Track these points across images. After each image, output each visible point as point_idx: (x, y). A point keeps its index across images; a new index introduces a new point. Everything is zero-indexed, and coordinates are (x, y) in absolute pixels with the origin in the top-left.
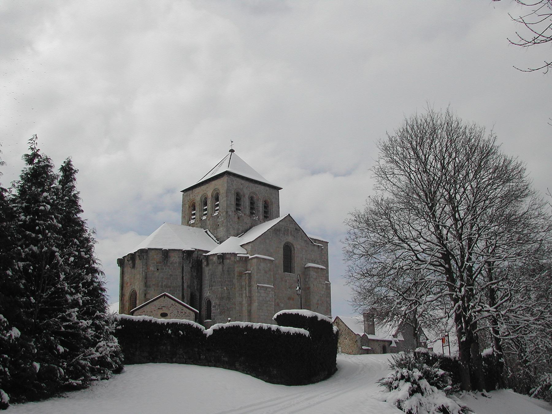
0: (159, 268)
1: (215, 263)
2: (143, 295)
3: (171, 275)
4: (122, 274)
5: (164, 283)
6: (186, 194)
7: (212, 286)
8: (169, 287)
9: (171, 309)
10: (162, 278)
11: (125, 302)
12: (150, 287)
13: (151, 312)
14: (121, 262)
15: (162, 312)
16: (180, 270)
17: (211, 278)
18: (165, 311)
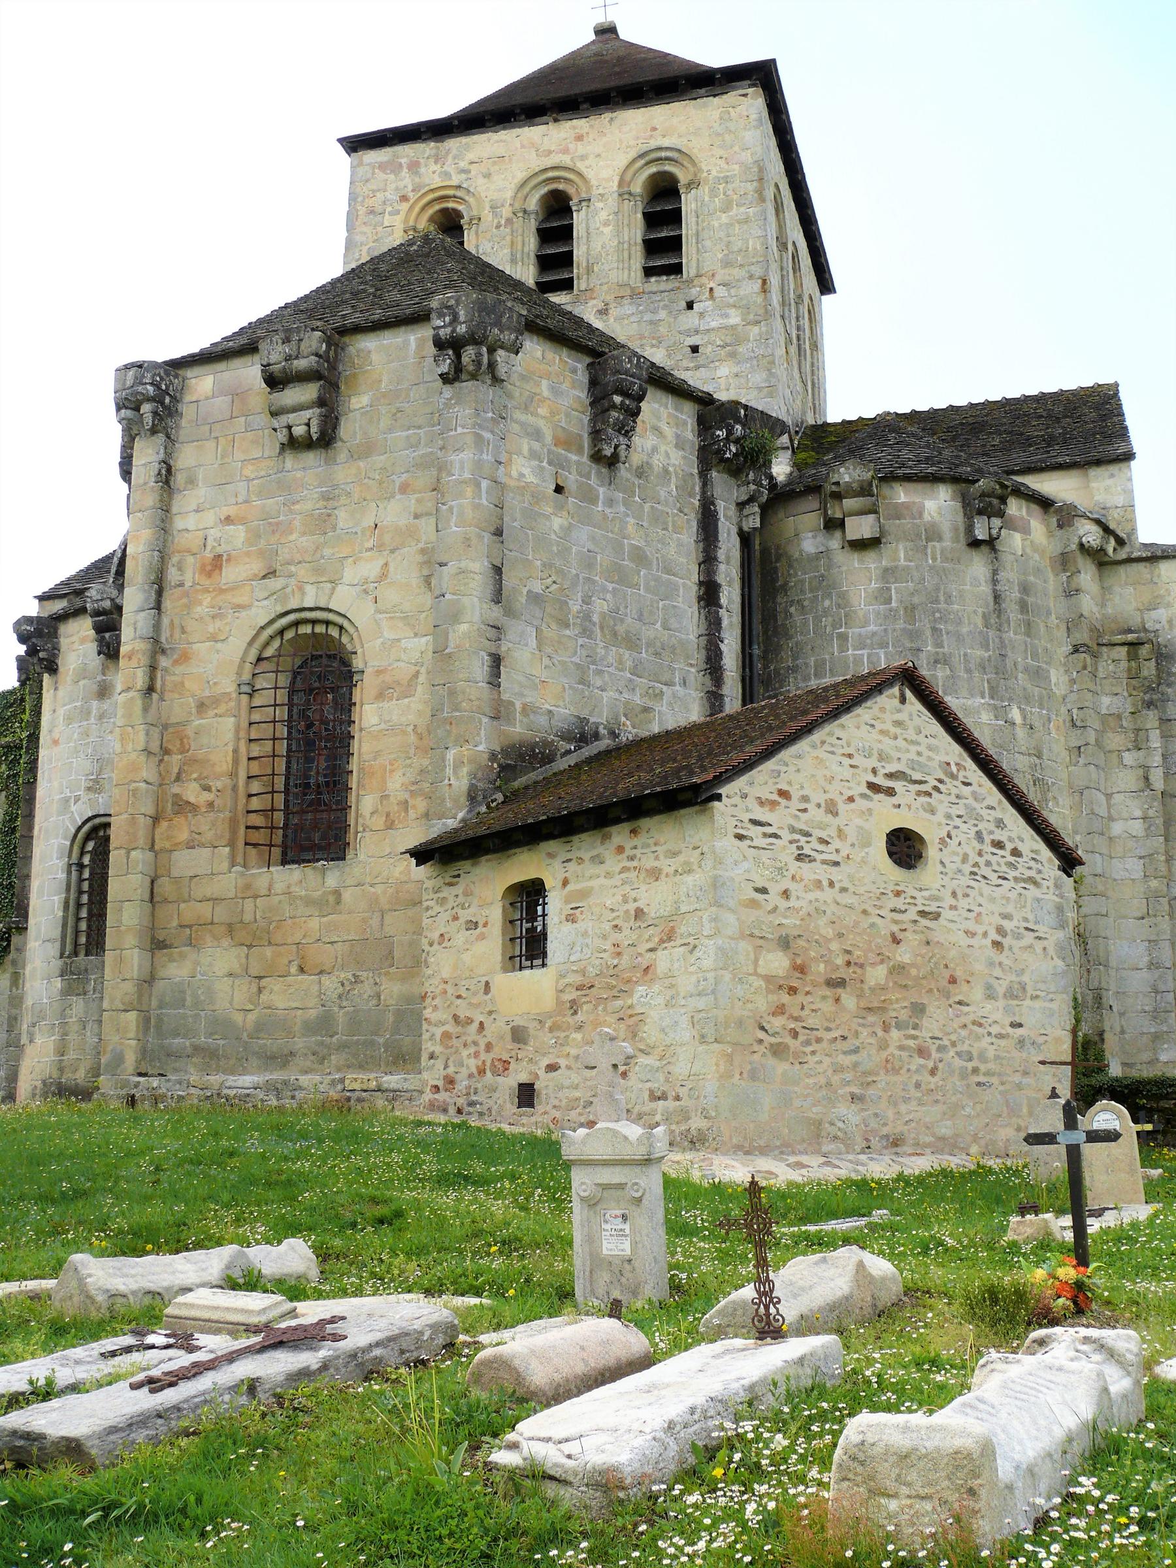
0: (571, 480)
1: (933, 534)
3: (640, 557)
5: (600, 606)
6: (373, 157)
8: (631, 642)
11: (178, 707)
13: (831, 809)
14: (152, 401)
16: (687, 535)
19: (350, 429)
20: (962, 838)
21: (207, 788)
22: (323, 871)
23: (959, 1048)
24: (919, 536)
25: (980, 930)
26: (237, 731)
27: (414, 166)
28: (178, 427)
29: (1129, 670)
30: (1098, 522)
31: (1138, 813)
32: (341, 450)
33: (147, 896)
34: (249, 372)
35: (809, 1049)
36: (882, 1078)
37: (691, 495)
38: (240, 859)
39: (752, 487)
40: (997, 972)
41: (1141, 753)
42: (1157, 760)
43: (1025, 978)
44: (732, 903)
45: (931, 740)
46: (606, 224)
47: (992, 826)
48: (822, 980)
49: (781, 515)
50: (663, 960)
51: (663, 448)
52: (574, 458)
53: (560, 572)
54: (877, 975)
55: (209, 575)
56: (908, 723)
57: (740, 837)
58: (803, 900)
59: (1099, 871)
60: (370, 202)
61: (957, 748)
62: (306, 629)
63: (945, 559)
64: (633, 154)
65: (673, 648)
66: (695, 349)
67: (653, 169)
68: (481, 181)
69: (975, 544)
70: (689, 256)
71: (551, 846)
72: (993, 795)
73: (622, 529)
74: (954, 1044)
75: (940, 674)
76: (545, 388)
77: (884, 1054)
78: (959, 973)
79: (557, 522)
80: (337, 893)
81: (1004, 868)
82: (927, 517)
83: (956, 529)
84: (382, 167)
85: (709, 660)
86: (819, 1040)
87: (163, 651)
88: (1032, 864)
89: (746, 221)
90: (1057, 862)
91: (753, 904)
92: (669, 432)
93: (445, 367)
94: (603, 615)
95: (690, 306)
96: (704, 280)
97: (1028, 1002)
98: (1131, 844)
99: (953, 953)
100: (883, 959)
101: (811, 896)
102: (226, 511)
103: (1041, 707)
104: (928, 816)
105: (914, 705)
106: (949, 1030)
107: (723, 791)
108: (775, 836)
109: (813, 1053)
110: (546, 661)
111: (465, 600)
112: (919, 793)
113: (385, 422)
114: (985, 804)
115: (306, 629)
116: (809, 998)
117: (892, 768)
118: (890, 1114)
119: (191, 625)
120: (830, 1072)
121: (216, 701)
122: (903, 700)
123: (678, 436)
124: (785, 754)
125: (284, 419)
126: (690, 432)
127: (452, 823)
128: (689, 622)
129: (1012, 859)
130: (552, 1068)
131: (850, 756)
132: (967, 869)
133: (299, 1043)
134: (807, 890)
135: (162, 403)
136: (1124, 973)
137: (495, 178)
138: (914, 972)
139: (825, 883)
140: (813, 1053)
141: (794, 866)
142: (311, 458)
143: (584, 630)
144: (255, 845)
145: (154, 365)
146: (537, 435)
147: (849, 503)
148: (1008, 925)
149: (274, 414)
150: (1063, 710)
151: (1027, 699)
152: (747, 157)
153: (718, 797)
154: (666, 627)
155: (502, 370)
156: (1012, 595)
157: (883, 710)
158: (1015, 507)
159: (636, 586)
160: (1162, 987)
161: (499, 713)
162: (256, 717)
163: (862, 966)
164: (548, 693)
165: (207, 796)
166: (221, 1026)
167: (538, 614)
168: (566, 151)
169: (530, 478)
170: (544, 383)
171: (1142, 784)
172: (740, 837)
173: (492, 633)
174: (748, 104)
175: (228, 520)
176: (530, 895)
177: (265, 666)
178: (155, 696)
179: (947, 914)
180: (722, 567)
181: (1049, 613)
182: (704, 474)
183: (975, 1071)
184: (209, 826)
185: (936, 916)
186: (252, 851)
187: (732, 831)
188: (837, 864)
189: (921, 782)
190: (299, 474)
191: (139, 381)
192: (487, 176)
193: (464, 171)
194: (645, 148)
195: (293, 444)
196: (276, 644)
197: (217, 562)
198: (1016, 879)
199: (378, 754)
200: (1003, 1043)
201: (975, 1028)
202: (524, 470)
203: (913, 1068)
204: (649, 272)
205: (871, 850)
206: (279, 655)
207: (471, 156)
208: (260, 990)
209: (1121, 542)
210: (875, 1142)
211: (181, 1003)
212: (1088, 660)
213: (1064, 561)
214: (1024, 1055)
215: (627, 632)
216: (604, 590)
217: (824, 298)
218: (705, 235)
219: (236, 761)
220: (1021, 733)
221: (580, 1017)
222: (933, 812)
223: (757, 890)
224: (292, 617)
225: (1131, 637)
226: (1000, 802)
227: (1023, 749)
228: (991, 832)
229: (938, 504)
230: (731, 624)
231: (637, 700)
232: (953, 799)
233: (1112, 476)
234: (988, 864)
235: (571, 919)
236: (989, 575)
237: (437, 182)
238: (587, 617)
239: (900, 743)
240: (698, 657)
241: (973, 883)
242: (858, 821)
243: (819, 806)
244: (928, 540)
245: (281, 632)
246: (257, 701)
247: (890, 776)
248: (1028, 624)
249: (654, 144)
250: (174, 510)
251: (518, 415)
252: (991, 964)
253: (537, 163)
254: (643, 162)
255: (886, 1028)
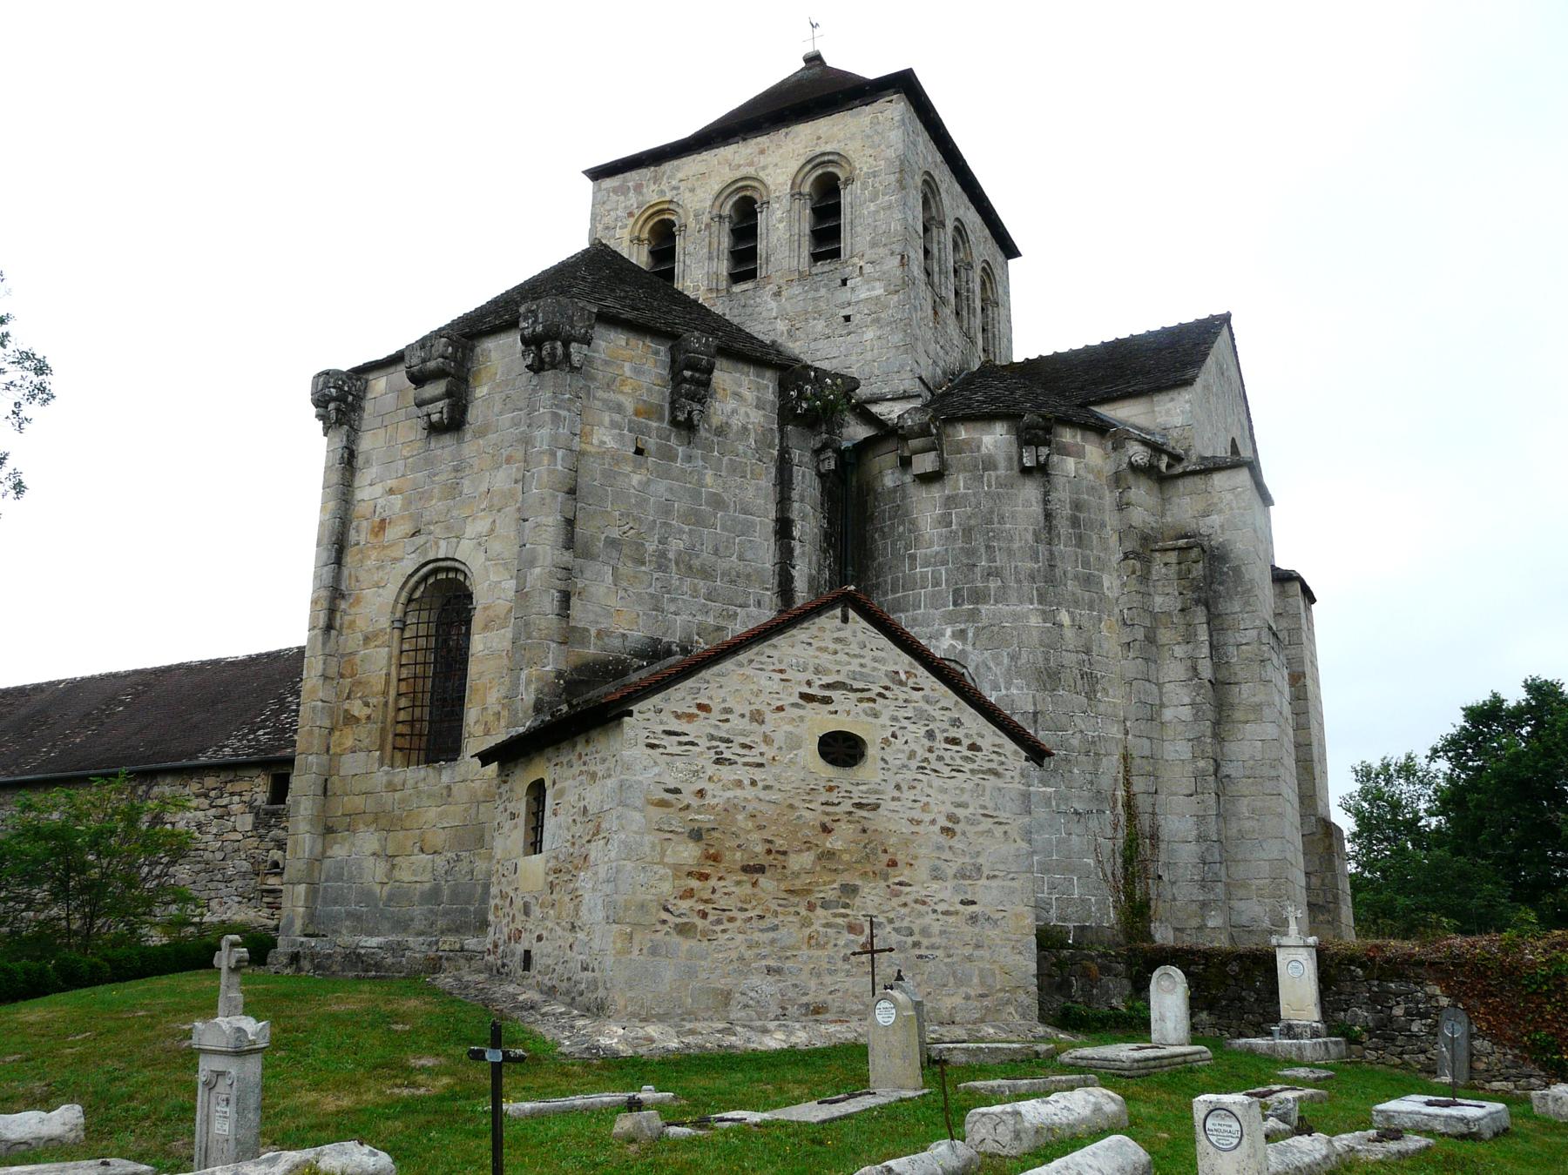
0: (651, 443)
1: (989, 464)
2: (548, 603)
3: (717, 502)
4: (347, 464)
5: (676, 545)
6: (609, 183)
7: (978, 597)
8: (706, 573)
9: (886, 709)
10: (666, 509)
11: (351, 641)
12: (587, 554)
13: (757, 717)
14: (340, 399)
15: (833, 726)
16: (766, 481)
17: (970, 553)
18: (846, 717)
19: (475, 414)
20: (910, 737)
21: (367, 705)
22: (440, 771)
23: (897, 925)
24: (976, 466)
25: (927, 818)
26: (390, 658)
27: (638, 188)
28: (361, 418)
29: (1180, 572)
30: (1145, 443)
31: (1187, 700)
32: (469, 431)
33: (320, 792)
34: (399, 375)
35: (719, 928)
36: (805, 952)
37: (771, 446)
38: (387, 761)
39: (825, 436)
40: (947, 855)
41: (1190, 646)
42: (1205, 651)
43: (980, 860)
44: (638, 803)
45: (877, 653)
46: (780, 221)
47: (946, 726)
48: (738, 867)
49: (870, 455)
50: (595, 850)
51: (742, 410)
52: (655, 424)
53: (637, 519)
54: (801, 861)
55: (376, 535)
56: (851, 639)
57: (652, 746)
58: (718, 796)
59: (1147, 753)
60: (606, 220)
61: (906, 658)
62: (442, 576)
63: (1000, 485)
64: (803, 161)
65: (749, 575)
66: (847, 319)
67: (820, 171)
68: (687, 194)
69: (1026, 471)
70: (846, 243)
71: (549, 752)
72: (948, 696)
73: (699, 480)
74: (891, 921)
75: (992, 585)
76: (627, 369)
77: (807, 931)
78: (900, 857)
79: (636, 479)
80: (449, 788)
81: (959, 762)
82: (984, 450)
83: (1010, 459)
84: (615, 191)
85: (780, 584)
86: (731, 920)
87: (343, 597)
88: (994, 756)
89: (890, 207)
90: (1024, 754)
91: (663, 804)
92: (750, 396)
93: (529, 361)
94: (679, 553)
95: (844, 282)
96: (856, 260)
97: (984, 881)
98: (1180, 728)
99: (893, 840)
100: (808, 845)
101: (730, 794)
102: (390, 483)
103: (1091, 608)
104: (870, 719)
105: (857, 622)
106: (885, 908)
107: (635, 708)
108: (692, 744)
109: (724, 931)
110: (621, 593)
111: (539, 548)
112: (861, 700)
113: (498, 407)
114: (940, 705)
115: (442, 576)
116: (722, 883)
117: (827, 680)
118: (813, 984)
119: (363, 575)
120: (743, 949)
121: (376, 635)
122: (845, 619)
123: (758, 398)
124: (706, 674)
125: (425, 409)
126: (770, 395)
127: (521, 730)
128: (766, 555)
129: (969, 754)
130: (540, 938)
131: (781, 671)
132: (914, 764)
133: (417, 910)
134: (725, 788)
135: (345, 401)
136: (1175, 846)
137: (698, 191)
138: (846, 857)
139: (747, 782)
140: (724, 931)
141: (711, 769)
142: (447, 439)
143: (660, 567)
144: (401, 749)
145: (337, 373)
146: (619, 408)
147: (914, 443)
148: (960, 812)
149: (419, 405)
150: (1116, 610)
151: (1076, 603)
152: (891, 153)
153: (630, 714)
154: (741, 558)
155: (576, 359)
156: (1064, 512)
157: (822, 629)
158: (1067, 436)
159: (714, 526)
160: (1209, 859)
161: (569, 636)
162: (406, 647)
163: (784, 853)
164: (617, 615)
165: (367, 711)
166: (367, 896)
167: (615, 554)
168: (751, 164)
169: (611, 444)
170: (627, 366)
171: (1191, 674)
172: (652, 746)
173: (562, 574)
174: (895, 109)
175: (391, 491)
176: (537, 791)
177: (413, 606)
178: (333, 633)
179: (888, 805)
180: (796, 505)
181: (1103, 525)
182: (781, 430)
183: (916, 945)
184: (366, 734)
185: (876, 807)
186: (398, 755)
187: (642, 741)
188: (761, 765)
189: (863, 690)
190: (439, 452)
191: (325, 385)
192: (692, 190)
193: (677, 188)
194: (812, 155)
195: (435, 429)
196: (422, 588)
197: (383, 525)
198: (972, 771)
199: (481, 674)
200: (951, 919)
201: (918, 906)
202: (605, 437)
203: (841, 942)
204: (816, 257)
205: (801, 752)
206: (422, 597)
207: (680, 175)
208: (393, 866)
209: (1176, 459)
210: (792, 1010)
211: (340, 877)
212: (1138, 565)
213: (1117, 480)
214: (977, 930)
215: (702, 565)
216: (681, 531)
217: (1010, 262)
218: (857, 221)
219: (387, 683)
220: (1069, 633)
221: (554, 896)
222: (876, 716)
223: (668, 791)
224: (431, 566)
225: (1181, 542)
226: (956, 703)
227: (1071, 647)
228: (945, 731)
229: (995, 439)
230: (803, 553)
231: (711, 620)
232: (901, 703)
233: (1172, 400)
234: (940, 758)
235: (555, 815)
236: (1040, 497)
237: (655, 199)
238: (662, 555)
239: (841, 657)
240: (773, 582)
241: (920, 777)
242: (789, 728)
243: (743, 716)
244: (985, 469)
245: (425, 578)
246: (407, 635)
247: (828, 686)
248: (1080, 538)
249: (818, 150)
250: (356, 484)
251: (600, 394)
252: (939, 848)
253: (729, 176)
254: (809, 167)
255: (811, 907)
